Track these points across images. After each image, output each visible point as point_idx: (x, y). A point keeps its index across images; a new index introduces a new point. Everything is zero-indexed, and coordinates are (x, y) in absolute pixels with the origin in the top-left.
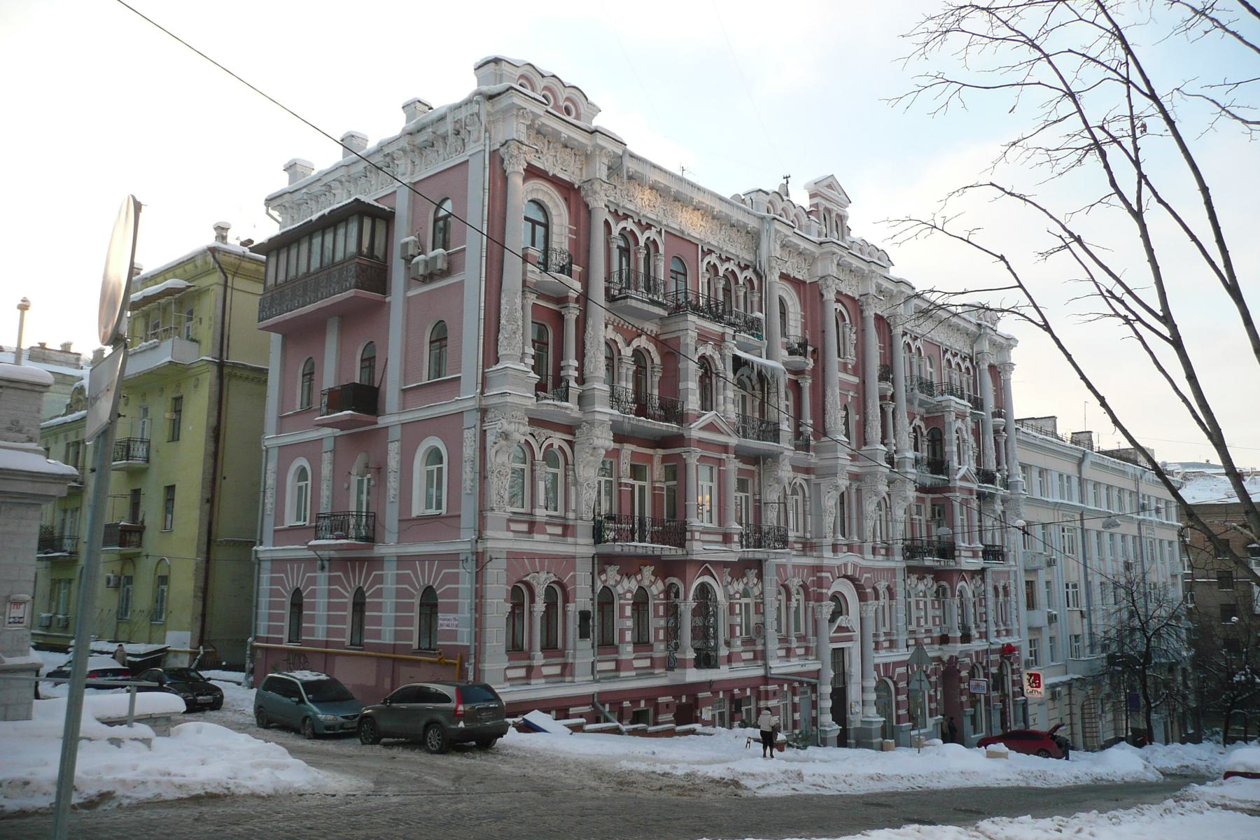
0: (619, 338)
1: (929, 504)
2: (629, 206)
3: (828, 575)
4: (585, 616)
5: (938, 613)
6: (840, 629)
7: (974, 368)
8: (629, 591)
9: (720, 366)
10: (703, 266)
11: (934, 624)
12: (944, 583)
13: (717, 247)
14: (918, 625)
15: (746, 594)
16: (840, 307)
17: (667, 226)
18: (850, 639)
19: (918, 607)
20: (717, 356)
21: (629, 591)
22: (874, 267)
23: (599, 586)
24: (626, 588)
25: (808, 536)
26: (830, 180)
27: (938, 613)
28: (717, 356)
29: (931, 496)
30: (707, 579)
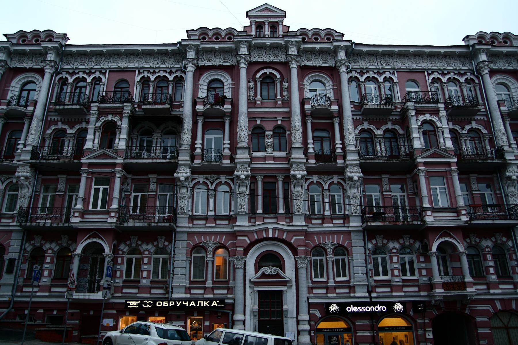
0: (66, 127)
1: (409, 182)
2: (80, 67)
3: (246, 238)
4: (12, 261)
5: (423, 265)
6: (264, 275)
7: (478, 78)
8: (50, 249)
9: (119, 123)
10: (138, 79)
11: (420, 274)
12: (426, 241)
13: (151, 68)
14: (393, 275)
15: (159, 251)
16: (268, 71)
17: (110, 68)
18: (285, 283)
19: (391, 261)
20: (116, 119)
21: (50, 249)
22: (286, 39)
23: (29, 248)
24: (51, 248)
25: (232, 213)
26: (265, 7)
27: (423, 265)
28: (116, 119)
29: (408, 176)
30: (95, 240)
